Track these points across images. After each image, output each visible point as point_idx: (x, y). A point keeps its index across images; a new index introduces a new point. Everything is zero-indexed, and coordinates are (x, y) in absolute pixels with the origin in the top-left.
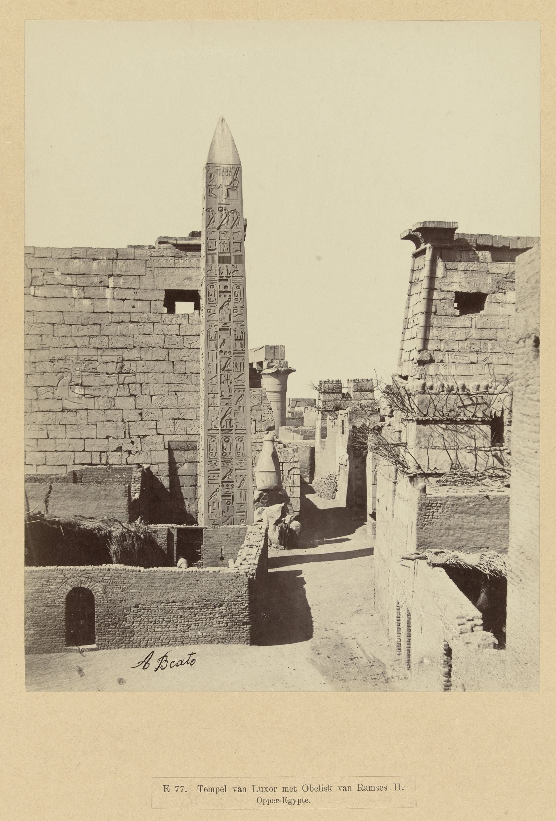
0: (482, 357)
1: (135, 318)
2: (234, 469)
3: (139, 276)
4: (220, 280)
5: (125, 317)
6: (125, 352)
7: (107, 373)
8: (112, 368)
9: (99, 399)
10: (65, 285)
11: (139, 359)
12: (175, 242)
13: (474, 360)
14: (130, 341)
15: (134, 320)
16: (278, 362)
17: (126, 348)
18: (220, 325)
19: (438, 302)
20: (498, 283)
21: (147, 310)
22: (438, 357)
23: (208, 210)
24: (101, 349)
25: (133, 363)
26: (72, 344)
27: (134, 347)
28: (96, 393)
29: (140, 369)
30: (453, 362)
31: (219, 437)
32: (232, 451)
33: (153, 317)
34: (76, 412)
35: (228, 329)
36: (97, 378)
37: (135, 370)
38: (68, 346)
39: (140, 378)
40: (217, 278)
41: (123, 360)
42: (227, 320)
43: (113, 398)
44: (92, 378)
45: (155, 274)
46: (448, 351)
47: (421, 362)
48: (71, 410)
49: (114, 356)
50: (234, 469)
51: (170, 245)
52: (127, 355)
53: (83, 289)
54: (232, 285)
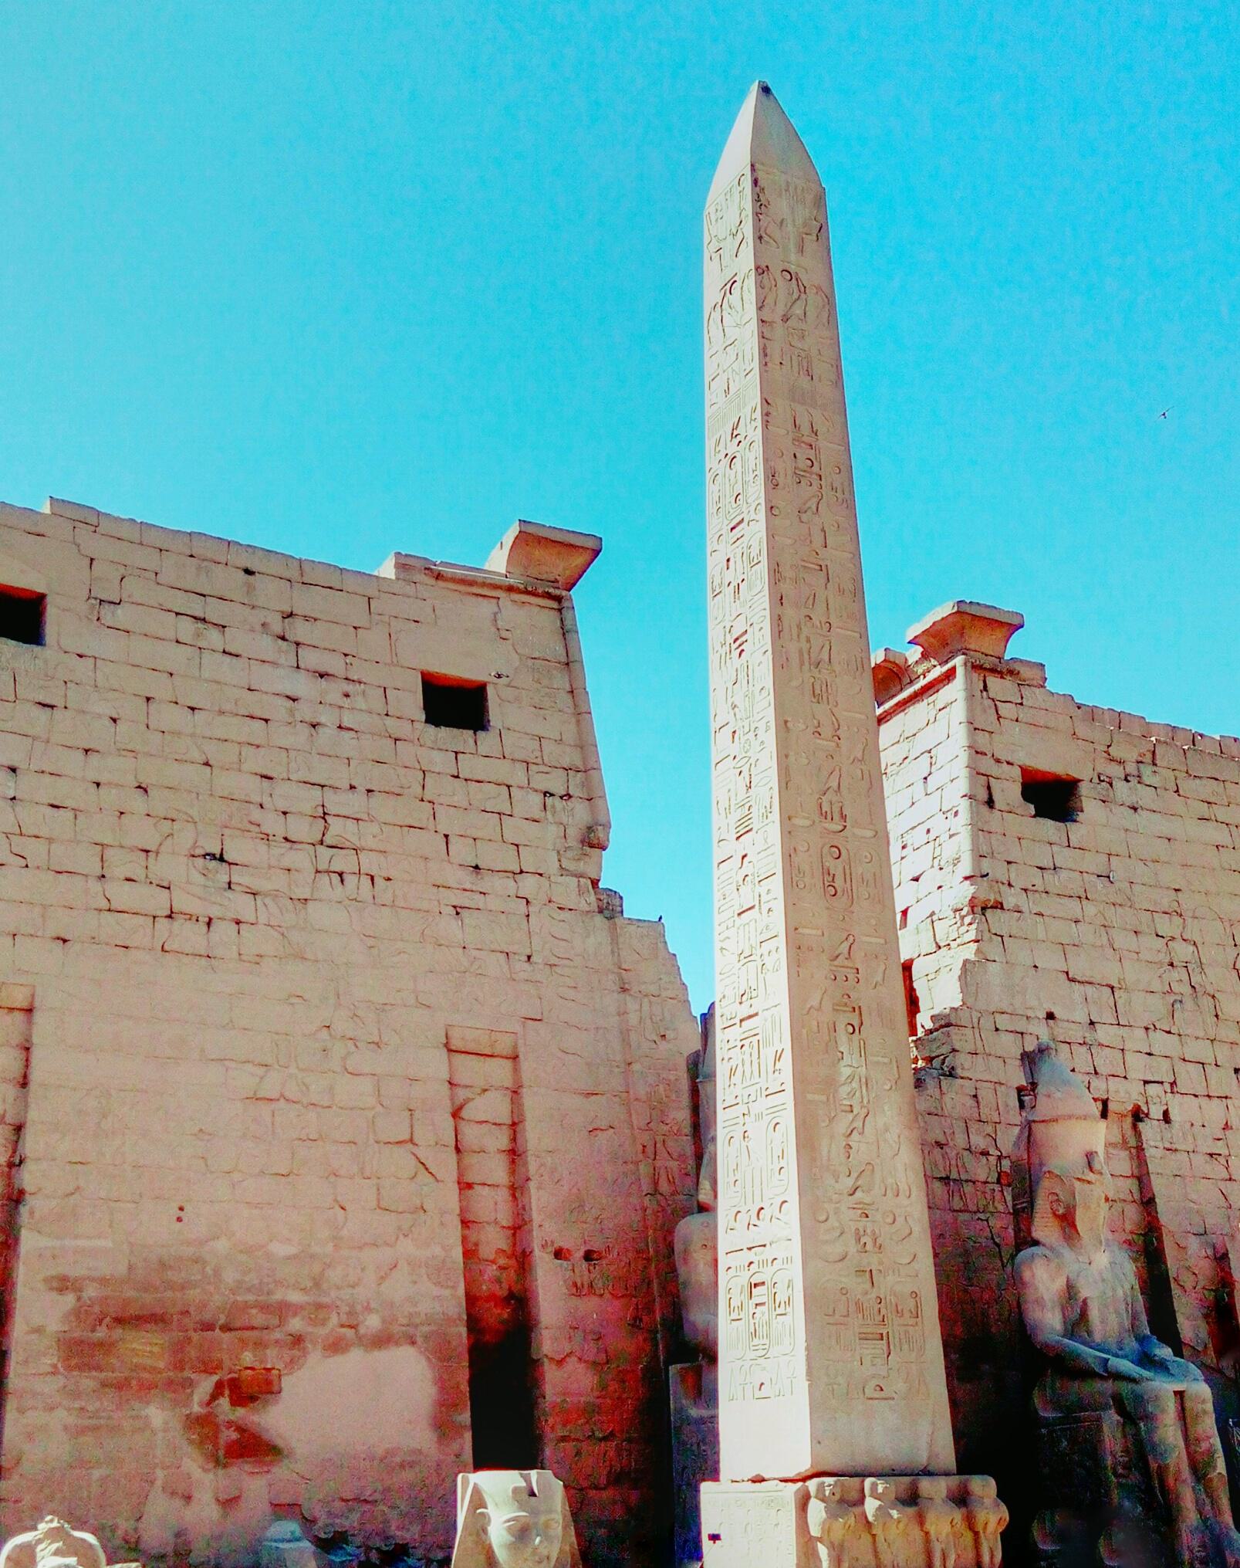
0: (1090, 909)
7: (286, 839)
22: (1010, 899)
27: (352, 787)
29: (370, 843)
34: (209, 924)
36: (262, 847)
37: (355, 840)
49: (308, 800)
52: (336, 802)
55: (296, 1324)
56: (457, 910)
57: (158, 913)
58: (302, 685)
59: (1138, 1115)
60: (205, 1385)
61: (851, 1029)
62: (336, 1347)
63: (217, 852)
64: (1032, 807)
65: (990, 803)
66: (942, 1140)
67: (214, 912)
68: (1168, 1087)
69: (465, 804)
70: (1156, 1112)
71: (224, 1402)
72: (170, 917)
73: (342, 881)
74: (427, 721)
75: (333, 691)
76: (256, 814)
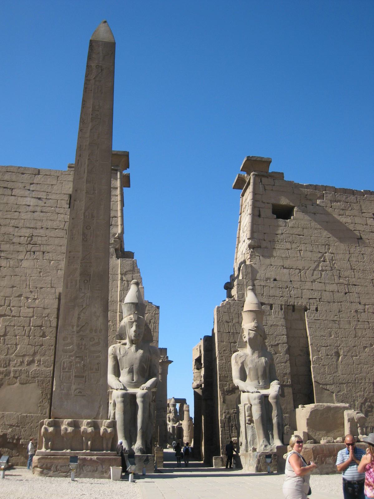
0: (294, 246)
1: (45, 209)
3: (52, 185)
5: (39, 209)
6: (35, 231)
13: (290, 248)
14: (39, 224)
15: (44, 211)
21: (55, 205)
24: (18, 227)
25: (40, 238)
27: (42, 228)
28: (10, 256)
29: (44, 243)
33: (58, 210)
36: (12, 246)
37: (40, 242)
39: (43, 248)
41: (32, 236)
43: (22, 260)
44: (8, 246)
46: (270, 241)
52: (36, 232)
58: (33, 202)
59: (306, 309)
61: (86, 281)
64: (275, 216)
65: (259, 216)
66: (228, 320)
70: (313, 308)
73: (34, 254)
75: (41, 203)
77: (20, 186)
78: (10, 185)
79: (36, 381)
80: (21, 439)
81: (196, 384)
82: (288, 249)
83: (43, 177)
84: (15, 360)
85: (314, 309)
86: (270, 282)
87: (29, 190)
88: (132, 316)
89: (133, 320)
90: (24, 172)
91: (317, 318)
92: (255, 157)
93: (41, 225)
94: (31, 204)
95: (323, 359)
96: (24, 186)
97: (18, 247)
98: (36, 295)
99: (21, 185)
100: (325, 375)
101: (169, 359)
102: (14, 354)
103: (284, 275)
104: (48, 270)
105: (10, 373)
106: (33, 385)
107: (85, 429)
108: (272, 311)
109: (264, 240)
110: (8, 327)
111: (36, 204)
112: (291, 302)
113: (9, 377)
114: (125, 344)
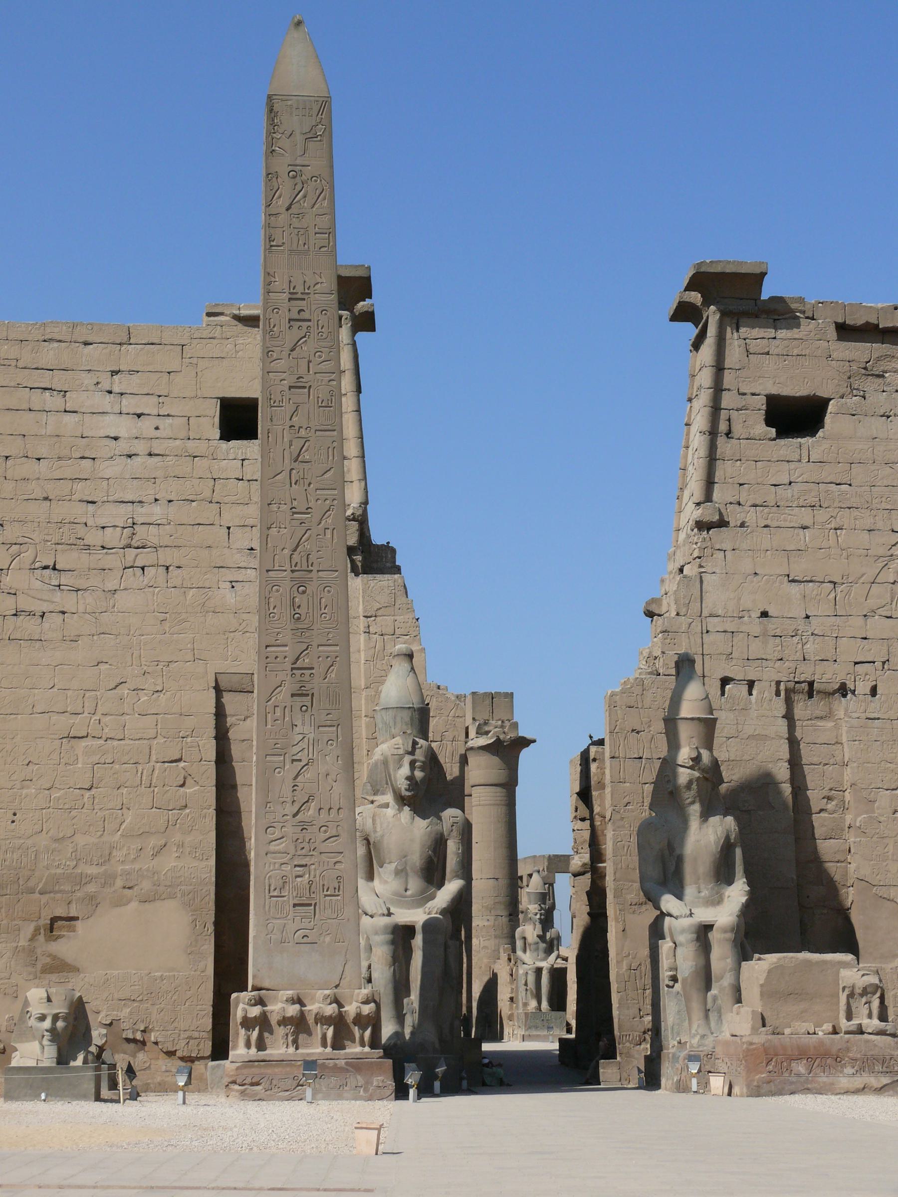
0: (821, 515)
2: (315, 644)
4: (290, 299)
5: (140, 447)
6: (139, 510)
7: (103, 548)
8: (112, 537)
9: (87, 594)
10: (31, 389)
11: (164, 521)
12: (236, 312)
15: (156, 452)
16: (500, 722)
17: (140, 502)
18: (291, 380)
19: (734, 414)
20: (849, 378)
21: (183, 434)
23: (270, 175)
24: (94, 502)
26: (40, 494)
27: (156, 500)
28: (81, 583)
29: (166, 541)
30: (766, 526)
31: (286, 585)
32: (311, 611)
34: (42, 616)
35: (304, 387)
36: (84, 555)
37: (155, 541)
38: (31, 497)
39: (165, 557)
40: (286, 296)
42: (303, 370)
44: (75, 554)
45: (199, 370)
46: (755, 506)
47: (702, 526)
48: (31, 614)
50: (315, 644)
51: (228, 318)
52: (141, 514)
53: (64, 396)
54: (313, 309)
55: (91, 888)
56: (233, 584)
57: (7, 613)
58: (123, 427)
59: (843, 690)
60: (30, 928)
61: (304, 708)
62: (120, 902)
63: (52, 564)
65: (728, 434)
67: (45, 607)
68: (878, 665)
69: (246, 500)
70: (863, 688)
71: (41, 938)
72: (15, 615)
74: (221, 439)
75: (146, 426)
76: (81, 531)
77: (86, 382)
78: (58, 380)
79: (179, 895)
80: (152, 1030)
81: (580, 863)
82: (805, 528)
83: (142, 349)
84: (124, 846)
85: (868, 691)
86: (751, 622)
87: (110, 392)
88: (398, 740)
89: (401, 752)
90: (90, 340)
91: (872, 716)
92: (720, 261)
93: (152, 492)
94: (122, 433)
95: (884, 821)
96: (100, 386)
97: (101, 556)
98: (159, 681)
99: (88, 380)
100: (885, 864)
101: (523, 732)
102: (119, 833)
103: (790, 602)
104: (184, 616)
105: (113, 877)
106: (171, 904)
107: (320, 1008)
108: (753, 698)
109: (740, 504)
110: (98, 768)
111: (135, 432)
112: (806, 673)
113: (113, 889)
114: (386, 806)
